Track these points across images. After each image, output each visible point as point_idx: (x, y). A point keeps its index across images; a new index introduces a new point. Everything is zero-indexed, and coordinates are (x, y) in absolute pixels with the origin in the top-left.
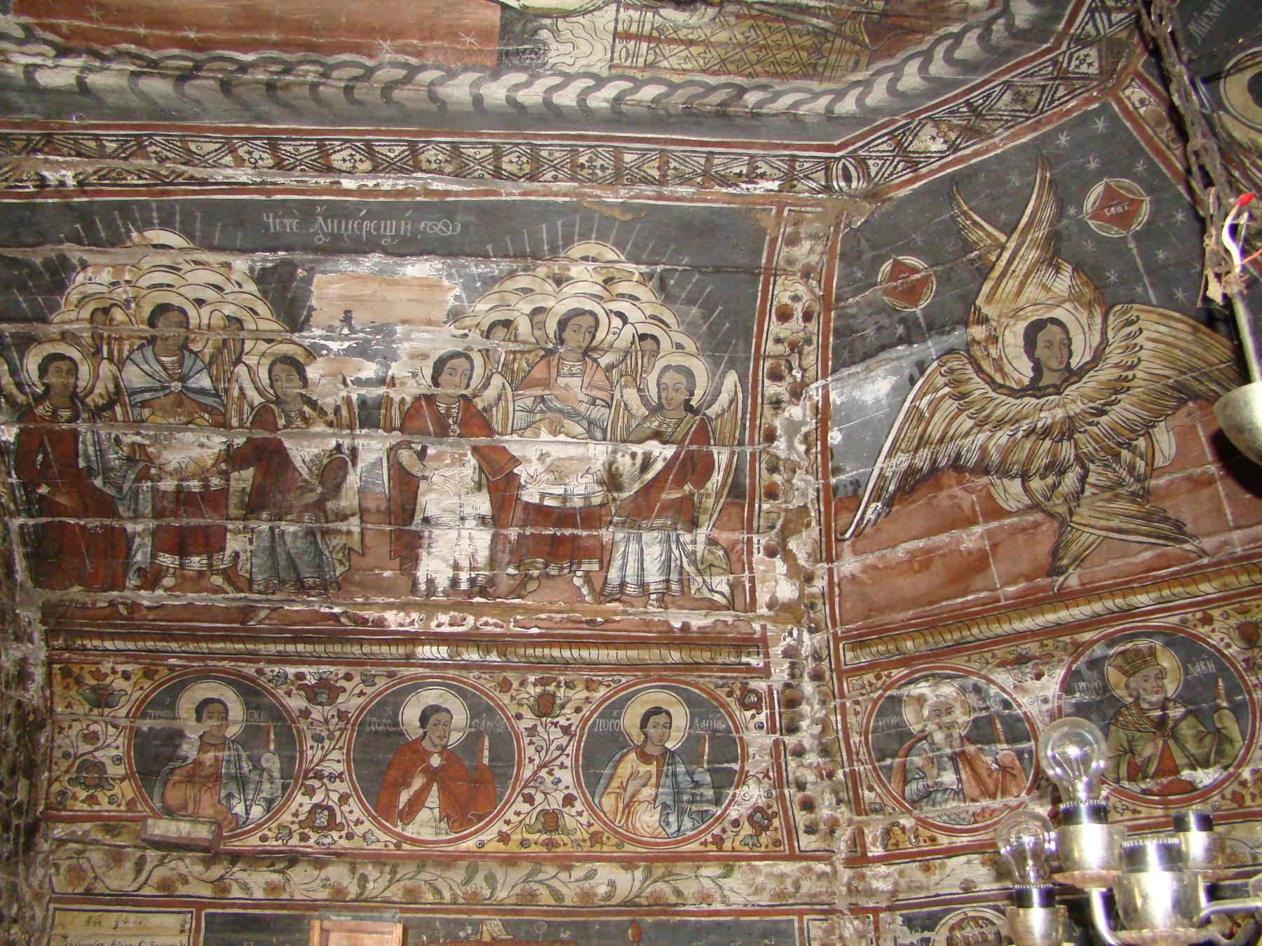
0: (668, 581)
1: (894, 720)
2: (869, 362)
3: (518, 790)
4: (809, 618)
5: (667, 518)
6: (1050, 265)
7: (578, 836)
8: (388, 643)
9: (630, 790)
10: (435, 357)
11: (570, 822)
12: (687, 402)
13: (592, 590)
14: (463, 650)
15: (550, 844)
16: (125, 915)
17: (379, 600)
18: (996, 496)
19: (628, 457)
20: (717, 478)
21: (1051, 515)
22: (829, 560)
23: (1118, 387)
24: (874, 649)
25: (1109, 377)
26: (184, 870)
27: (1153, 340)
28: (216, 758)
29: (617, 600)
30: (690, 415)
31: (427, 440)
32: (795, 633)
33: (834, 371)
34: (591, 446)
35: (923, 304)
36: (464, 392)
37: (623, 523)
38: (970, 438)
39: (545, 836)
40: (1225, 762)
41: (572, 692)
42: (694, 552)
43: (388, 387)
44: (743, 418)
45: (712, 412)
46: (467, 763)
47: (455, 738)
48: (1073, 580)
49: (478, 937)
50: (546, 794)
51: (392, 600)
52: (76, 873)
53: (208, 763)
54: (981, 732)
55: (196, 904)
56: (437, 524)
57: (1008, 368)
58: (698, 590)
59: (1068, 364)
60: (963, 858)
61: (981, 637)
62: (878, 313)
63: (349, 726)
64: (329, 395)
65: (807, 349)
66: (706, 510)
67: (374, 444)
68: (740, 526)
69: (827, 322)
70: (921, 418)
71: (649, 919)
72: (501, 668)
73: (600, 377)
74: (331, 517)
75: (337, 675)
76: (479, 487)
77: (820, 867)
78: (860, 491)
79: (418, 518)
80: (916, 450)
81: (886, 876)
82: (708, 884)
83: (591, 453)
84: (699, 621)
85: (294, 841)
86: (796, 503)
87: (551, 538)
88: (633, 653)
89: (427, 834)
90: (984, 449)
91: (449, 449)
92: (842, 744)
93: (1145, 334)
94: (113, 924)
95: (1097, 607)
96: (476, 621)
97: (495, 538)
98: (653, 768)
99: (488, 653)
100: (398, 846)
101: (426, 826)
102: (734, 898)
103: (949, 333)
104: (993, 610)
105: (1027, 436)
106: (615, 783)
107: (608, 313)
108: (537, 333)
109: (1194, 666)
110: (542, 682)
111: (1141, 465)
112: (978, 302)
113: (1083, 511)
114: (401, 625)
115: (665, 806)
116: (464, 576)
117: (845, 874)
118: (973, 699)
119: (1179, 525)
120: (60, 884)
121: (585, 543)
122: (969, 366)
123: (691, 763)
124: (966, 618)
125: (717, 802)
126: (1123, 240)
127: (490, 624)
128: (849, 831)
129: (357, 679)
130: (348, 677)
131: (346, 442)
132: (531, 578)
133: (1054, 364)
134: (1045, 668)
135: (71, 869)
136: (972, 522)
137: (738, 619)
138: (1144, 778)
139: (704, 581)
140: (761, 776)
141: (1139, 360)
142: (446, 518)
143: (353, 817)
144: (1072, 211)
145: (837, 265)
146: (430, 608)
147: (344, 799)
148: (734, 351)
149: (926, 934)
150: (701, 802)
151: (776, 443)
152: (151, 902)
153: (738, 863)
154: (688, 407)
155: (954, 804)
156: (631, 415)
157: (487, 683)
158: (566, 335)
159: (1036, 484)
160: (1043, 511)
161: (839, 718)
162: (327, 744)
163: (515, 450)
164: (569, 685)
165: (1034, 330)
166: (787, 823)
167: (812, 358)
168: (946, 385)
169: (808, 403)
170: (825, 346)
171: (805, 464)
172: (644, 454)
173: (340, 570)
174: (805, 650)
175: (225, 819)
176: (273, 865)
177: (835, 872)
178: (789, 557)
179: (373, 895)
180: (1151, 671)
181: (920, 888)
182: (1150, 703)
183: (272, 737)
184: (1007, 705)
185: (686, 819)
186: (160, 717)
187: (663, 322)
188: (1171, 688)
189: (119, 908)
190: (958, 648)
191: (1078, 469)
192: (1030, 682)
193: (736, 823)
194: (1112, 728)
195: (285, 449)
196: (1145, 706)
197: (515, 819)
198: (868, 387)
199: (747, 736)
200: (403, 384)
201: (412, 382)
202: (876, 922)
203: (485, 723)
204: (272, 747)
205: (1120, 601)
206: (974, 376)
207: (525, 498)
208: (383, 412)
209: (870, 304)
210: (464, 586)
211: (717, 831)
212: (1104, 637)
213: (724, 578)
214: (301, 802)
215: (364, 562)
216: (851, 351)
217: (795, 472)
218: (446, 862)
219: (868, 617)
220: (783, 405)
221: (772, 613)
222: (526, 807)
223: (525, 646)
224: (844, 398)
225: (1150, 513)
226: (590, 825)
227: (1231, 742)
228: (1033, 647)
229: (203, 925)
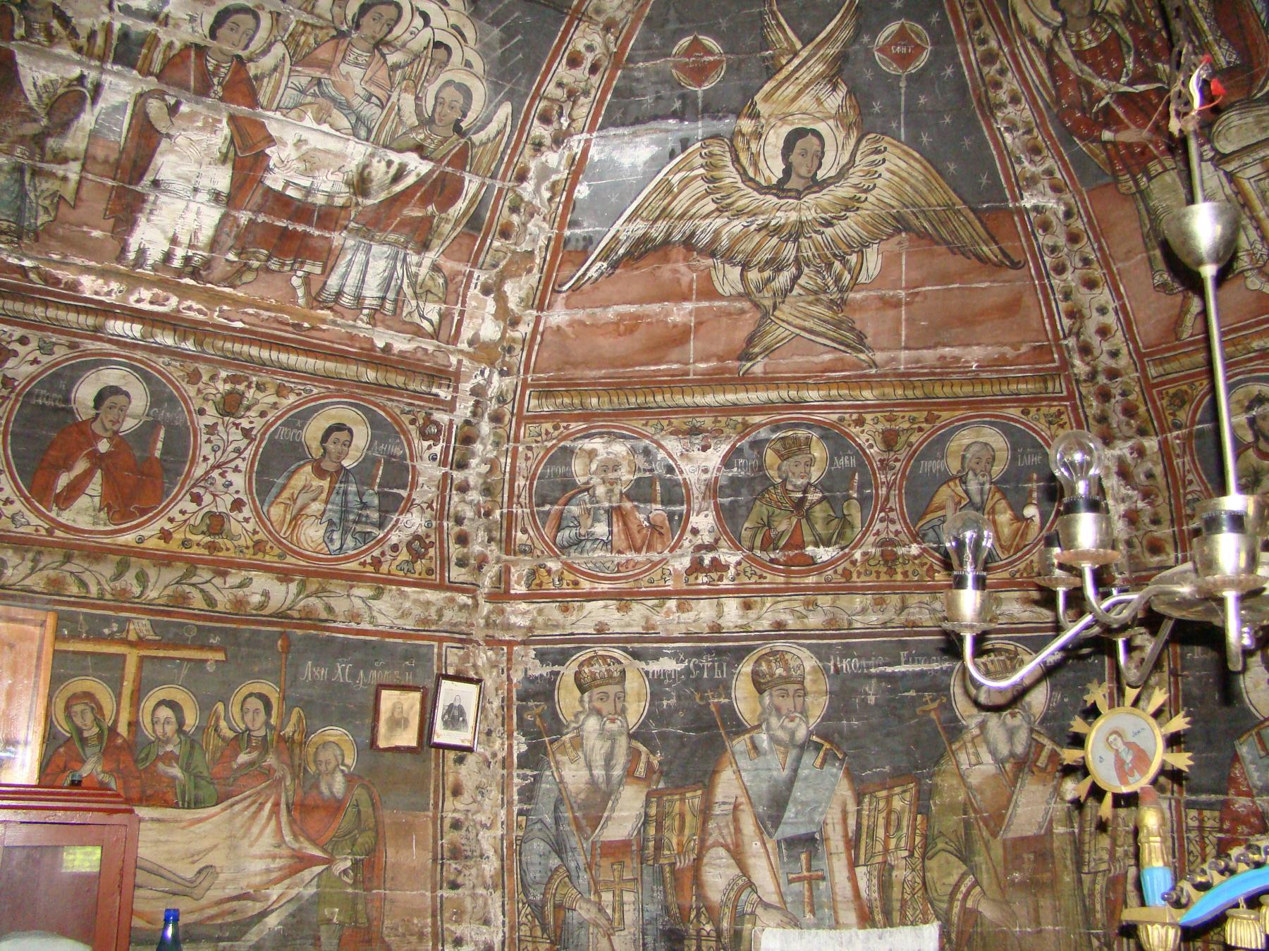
0: (384, 298)
1: (562, 470)
2: (637, 127)
3: (186, 488)
4: (503, 361)
5: (401, 234)
6: (830, 81)
7: (242, 542)
8: (78, 310)
9: (299, 503)
10: (220, 6)
11: (235, 527)
12: (458, 122)
13: (308, 293)
14: (158, 331)
15: (212, 547)
17: (79, 261)
18: (714, 278)
19: (383, 164)
20: (461, 205)
21: (757, 306)
22: (540, 308)
23: (850, 205)
24: (559, 401)
25: (845, 195)
27: (893, 173)
29: (329, 308)
30: (456, 136)
31: (183, 96)
32: (487, 373)
33: (601, 128)
34: (352, 144)
35: (706, 86)
36: (240, 53)
37: (358, 230)
38: (708, 221)
39: (208, 539)
40: (843, 543)
41: (262, 395)
42: (416, 275)
43: (160, 25)
44: (504, 152)
45: (476, 138)
46: (138, 454)
47: (129, 425)
48: (758, 368)
49: (124, 635)
50: (215, 496)
51: (93, 263)
54: (641, 492)
56: (166, 191)
57: (762, 165)
58: (410, 313)
59: (815, 174)
60: (601, 603)
61: (663, 404)
62: (663, 82)
63: (13, 396)
64: (88, 16)
65: (582, 100)
66: (441, 234)
67: (125, 85)
68: (466, 257)
69: (610, 79)
70: (670, 191)
71: (299, 632)
72: (194, 358)
73: (383, 74)
74: (49, 156)
75: (11, 336)
76: (224, 159)
77: (463, 599)
78: (590, 248)
79: (148, 178)
80: (655, 221)
81: (524, 613)
82: (358, 603)
83: (349, 151)
84: (402, 344)
86: (525, 247)
87: (282, 230)
88: (330, 365)
89: (84, 523)
90: (717, 233)
91: (205, 112)
92: (506, 486)
93: (887, 164)
95: (773, 395)
96: (179, 303)
97: (224, 218)
98: (325, 484)
99: (185, 339)
100: (50, 532)
101: (83, 514)
102: (381, 620)
103: (720, 119)
104: (678, 382)
105: (759, 230)
106: (286, 494)
107: (414, 9)
108: (337, 10)
109: (839, 458)
110: (233, 379)
111: (847, 277)
112: (756, 98)
113: (785, 307)
114: (97, 293)
115: (331, 522)
116: (180, 252)
117: (486, 608)
118: (640, 461)
119: (861, 337)
121: (311, 242)
122: (728, 155)
123: (363, 484)
124: (653, 385)
125: (381, 526)
126: (898, 78)
127: (193, 309)
128: (497, 568)
129: (34, 344)
130: (23, 341)
131: (92, 75)
132: (250, 268)
133: (803, 172)
134: (712, 442)
136: (686, 298)
137: (439, 349)
138: (775, 549)
139: (418, 306)
140: (425, 506)
141: (875, 186)
142: (179, 186)
144: (866, 39)
145: (640, 26)
146: (133, 280)
148: (517, 83)
149: (556, 668)
150: (366, 523)
151: (525, 184)
153: (389, 587)
154: (457, 129)
155: (602, 553)
156: (401, 122)
157: (175, 371)
158: (365, 21)
159: (753, 275)
160: (751, 301)
161: (509, 460)
163: (273, 129)
165: (796, 135)
166: (442, 553)
167: (585, 110)
168: (702, 166)
169: (567, 153)
170: (601, 102)
171: (544, 210)
172: (400, 164)
173: (43, 218)
174: (492, 391)
177: (476, 605)
178: (501, 299)
179: (10, 582)
180: (801, 458)
181: (557, 626)
182: (795, 486)
184: (670, 469)
185: (349, 537)
187: (462, 35)
188: (815, 474)
190: (640, 411)
191: (793, 270)
192: (696, 452)
193: (395, 548)
194: (758, 503)
195: (16, 64)
196: (790, 487)
198: (629, 151)
199: (420, 465)
200: (177, 26)
201: (187, 27)
202: (510, 653)
203: (164, 414)
205: (793, 393)
206: (730, 164)
207: (268, 183)
208: (144, 51)
209: (657, 73)
210: (177, 263)
211: (376, 553)
212: (770, 423)
213: (437, 307)
215: (73, 216)
216: (624, 113)
217: (532, 216)
218: (97, 554)
219: (559, 370)
220: (543, 149)
221: (471, 350)
222: (193, 507)
223: (225, 338)
224: (603, 156)
225: (841, 322)
226: (255, 532)
227: (853, 527)
228: (707, 422)
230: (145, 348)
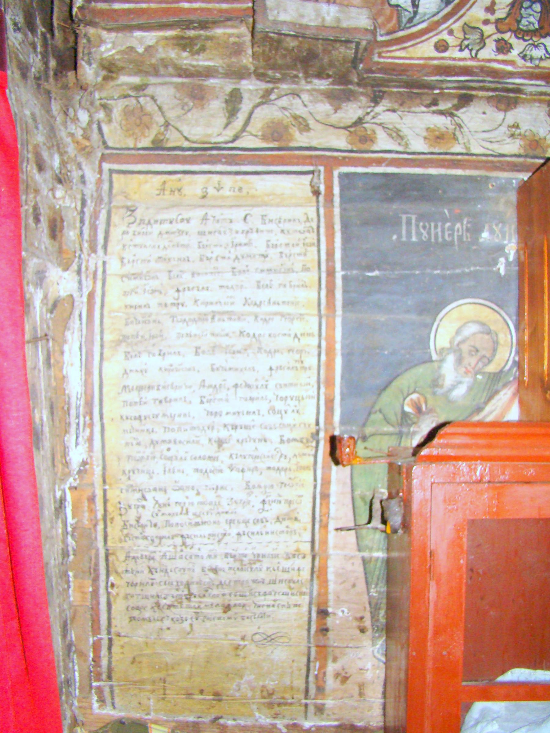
16: (216, 178)
26: (301, 111)
52: (137, 119)
55: (327, 160)
85: (488, 52)
94: (199, 192)
120: (114, 135)
135: (127, 113)
152: (252, 156)
176: (435, 103)
189: (206, 167)
229: (336, 190)
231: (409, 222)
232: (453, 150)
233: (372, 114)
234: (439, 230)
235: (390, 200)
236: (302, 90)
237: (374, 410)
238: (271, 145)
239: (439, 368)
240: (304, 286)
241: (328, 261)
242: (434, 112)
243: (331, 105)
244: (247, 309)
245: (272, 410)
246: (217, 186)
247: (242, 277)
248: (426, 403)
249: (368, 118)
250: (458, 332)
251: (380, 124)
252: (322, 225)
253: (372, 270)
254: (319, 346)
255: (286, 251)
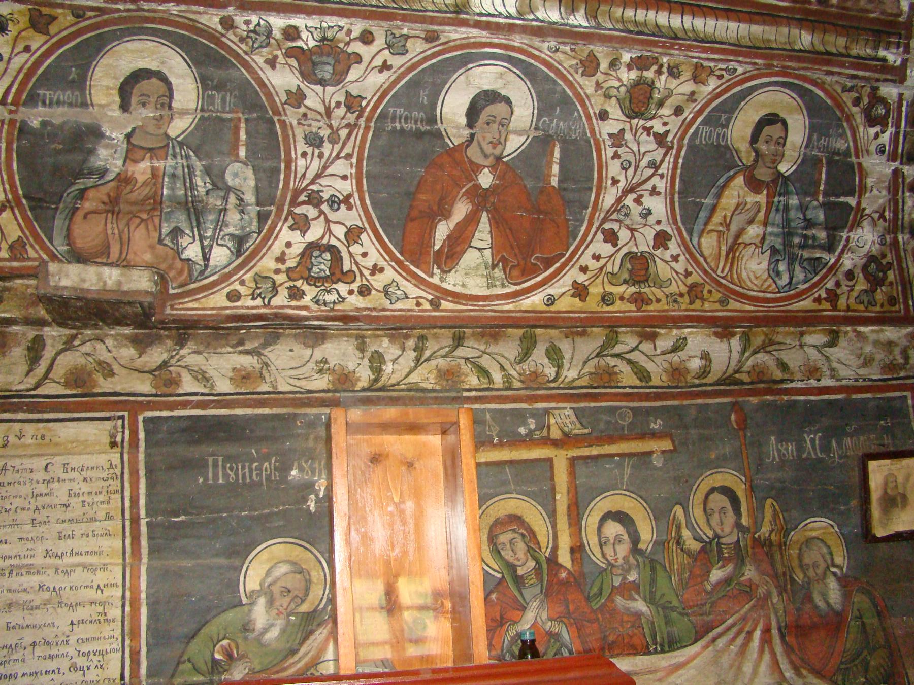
3: (596, 224)
7: (673, 289)
9: (734, 228)
11: (662, 270)
15: (639, 300)
16: (17, 426)
26: (105, 356)
28: (154, 172)
39: (633, 289)
47: (514, 144)
50: (632, 230)
53: (141, 179)
55: (130, 404)
63: (362, 121)
71: (754, 400)
72: (587, 37)
75: (349, 32)
82: (813, 353)
85: (281, 299)
89: (476, 286)
98: (762, 198)
99: (573, 10)
100: (435, 304)
102: (843, 372)
106: (717, 218)
110: (639, 64)
115: (774, 251)
123: (806, 194)
129: (380, 41)
130: (366, 38)
140: (876, 216)
143: (369, 262)
147: (353, 235)
150: (813, 247)
152: (55, 404)
153: (843, 328)
162: (327, 148)
164: (674, 72)
175: (171, 267)
176: (241, 343)
179: (393, 381)
183: (243, 136)
185: (798, 269)
186: (59, 103)
193: (850, 275)
197: (593, 265)
203: (557, 124)
204: (242, 153)
211: (830, 284)
214: (289, 241)
218: (493, 329)
222: (606, 249)
226: (688, 274)
229: (142, 435)
230: (524, 30)
231: (215, 465)
232: (259, 390)
233: (177, 357)
234: (247, 470)
235: (197, 442)
236: (107, 335)
237: (182, 659)
238: (74, 392)
239: (250, 611)
240: (108, 534)
241: (131, 507)
242: (241, 352)
243: (136, 350)
244: (48, 561)
245: (74, 668)
246: (19, 434)
247: (42, 528)
248: (237, 648)
249: (173, 361)
250: (268, 573)
251: (185, 367)
252: (126, 471)
253: (179, 517)
254: (123, 597)
255: (89, 499)
